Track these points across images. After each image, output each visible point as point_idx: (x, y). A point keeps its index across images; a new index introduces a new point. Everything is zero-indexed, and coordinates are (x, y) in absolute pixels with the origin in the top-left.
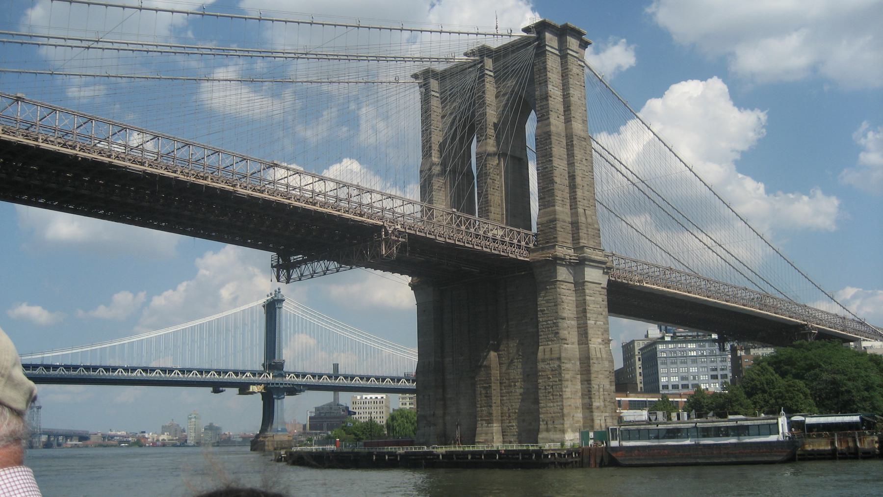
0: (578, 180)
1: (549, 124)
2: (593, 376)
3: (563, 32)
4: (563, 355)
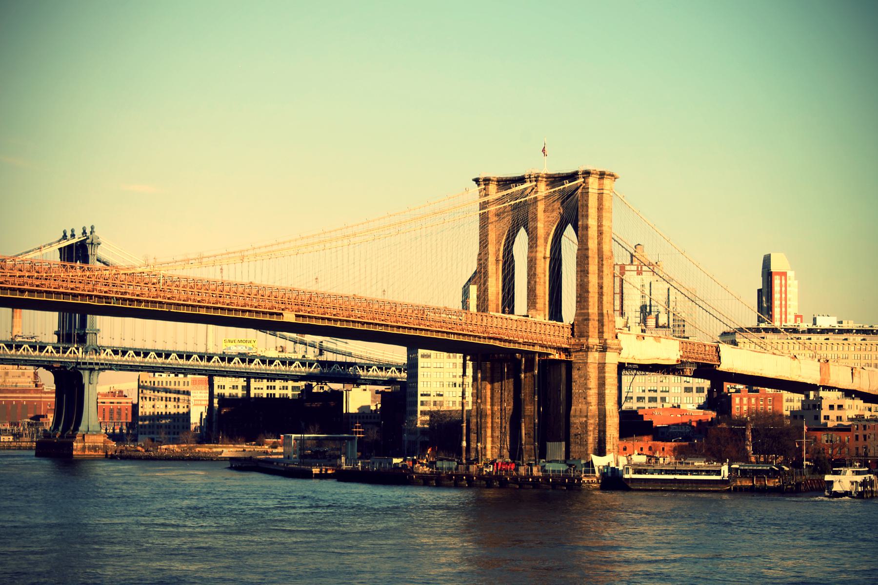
0: (605, 289)
1: (587, 249)
2: (607, 429)
3: (602, 175)
4: (589, 414)
